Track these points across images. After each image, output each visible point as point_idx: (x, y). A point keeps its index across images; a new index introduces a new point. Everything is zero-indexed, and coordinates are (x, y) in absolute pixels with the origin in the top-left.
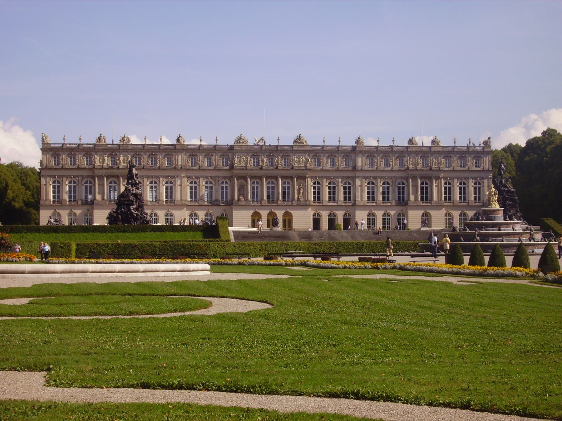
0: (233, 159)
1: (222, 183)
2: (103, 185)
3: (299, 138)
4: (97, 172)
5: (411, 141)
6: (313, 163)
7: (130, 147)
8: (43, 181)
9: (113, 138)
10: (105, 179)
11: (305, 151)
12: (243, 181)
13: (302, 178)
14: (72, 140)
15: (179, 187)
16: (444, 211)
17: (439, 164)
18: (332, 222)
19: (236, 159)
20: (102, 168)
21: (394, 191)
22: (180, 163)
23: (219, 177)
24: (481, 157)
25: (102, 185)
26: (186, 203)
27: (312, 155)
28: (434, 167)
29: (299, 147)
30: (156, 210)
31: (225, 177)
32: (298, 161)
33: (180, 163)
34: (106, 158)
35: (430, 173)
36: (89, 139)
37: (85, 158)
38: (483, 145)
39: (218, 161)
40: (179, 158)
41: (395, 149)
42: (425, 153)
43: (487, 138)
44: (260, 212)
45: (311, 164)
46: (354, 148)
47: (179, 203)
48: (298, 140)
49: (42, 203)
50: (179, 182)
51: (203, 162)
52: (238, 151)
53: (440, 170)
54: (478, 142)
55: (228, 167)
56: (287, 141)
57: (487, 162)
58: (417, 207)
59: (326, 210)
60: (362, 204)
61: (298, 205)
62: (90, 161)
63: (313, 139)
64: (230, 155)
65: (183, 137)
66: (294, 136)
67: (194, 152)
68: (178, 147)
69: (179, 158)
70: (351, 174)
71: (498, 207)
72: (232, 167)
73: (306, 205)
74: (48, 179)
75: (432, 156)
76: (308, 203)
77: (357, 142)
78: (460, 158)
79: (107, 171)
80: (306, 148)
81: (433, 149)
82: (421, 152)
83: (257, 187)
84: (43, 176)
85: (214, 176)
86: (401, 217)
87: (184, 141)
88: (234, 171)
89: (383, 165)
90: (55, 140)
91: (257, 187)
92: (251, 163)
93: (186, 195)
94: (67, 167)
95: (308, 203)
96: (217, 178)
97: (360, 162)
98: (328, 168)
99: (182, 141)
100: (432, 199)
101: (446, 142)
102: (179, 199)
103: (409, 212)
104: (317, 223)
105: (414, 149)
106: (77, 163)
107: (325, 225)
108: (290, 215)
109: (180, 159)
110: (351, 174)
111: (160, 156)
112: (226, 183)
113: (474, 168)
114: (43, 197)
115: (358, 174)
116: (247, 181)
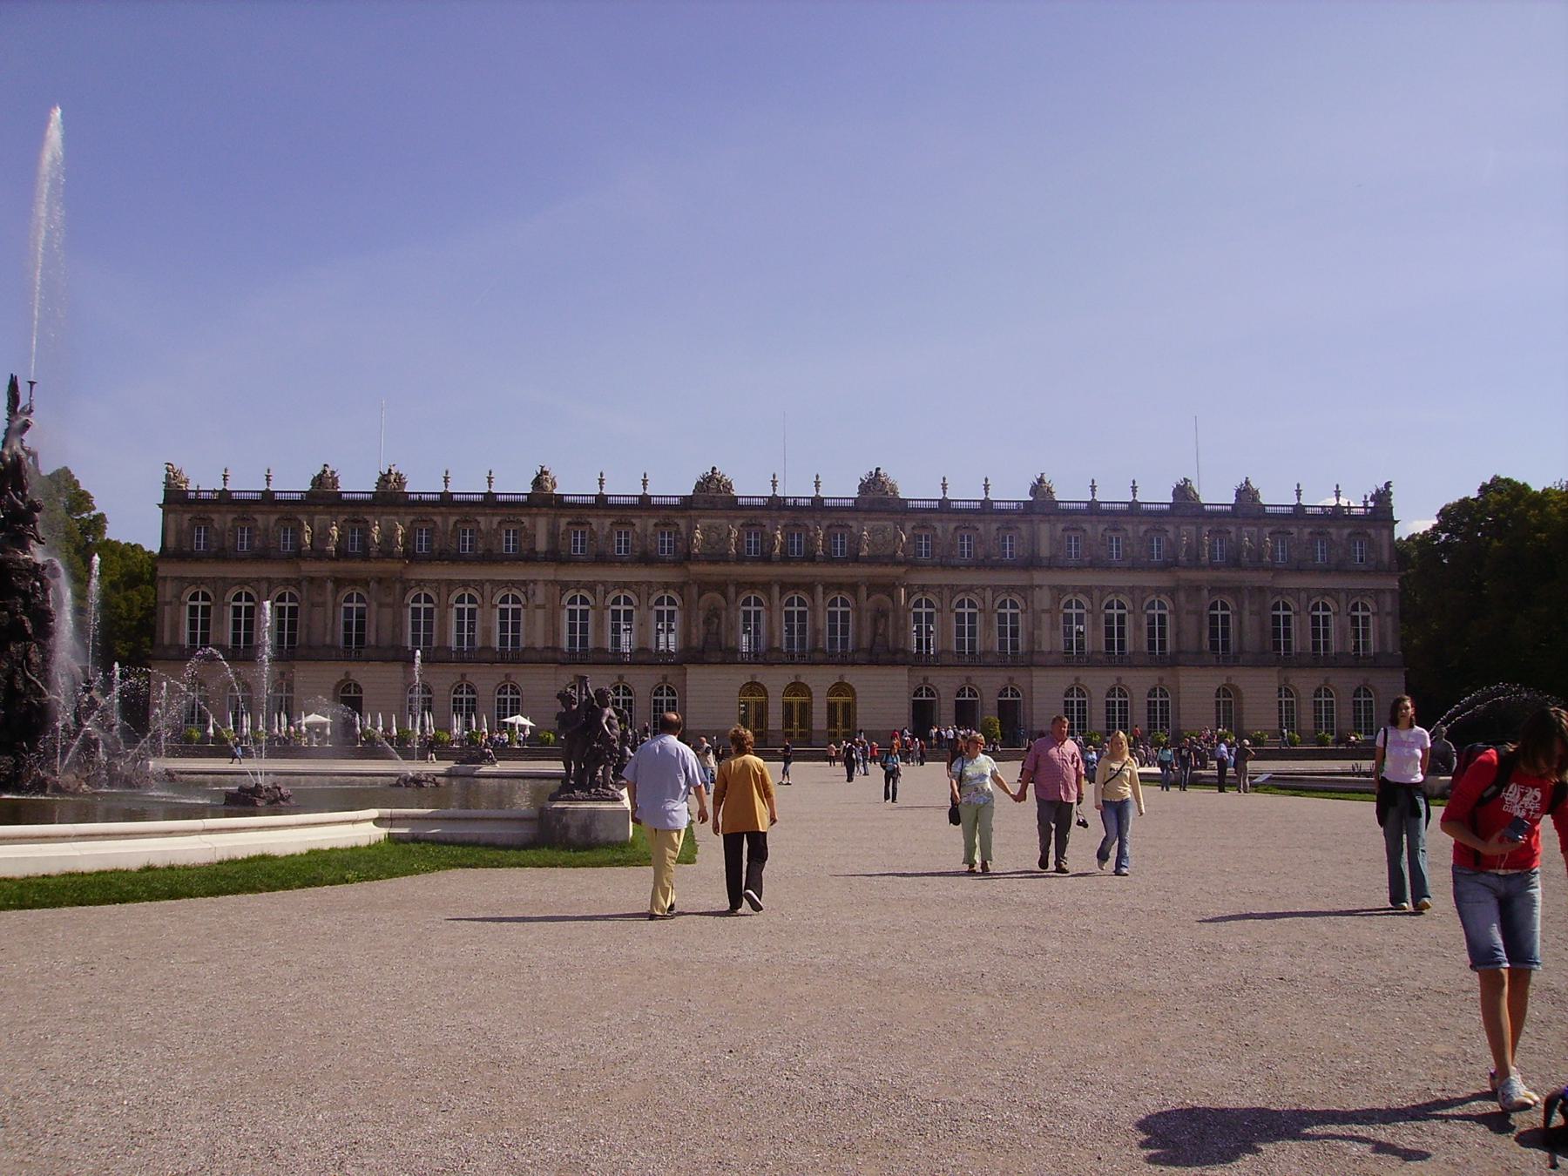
1: (660, 602)
21: (1138, 627)
22: (542, 545)
23: (650, 584)
26: (559, 656)
31: (667, 586)
33: (542, 545)
38: (1371, 504)
43: (1381, 486)
64: (682, 523)
65: (552, 474)
66: (863, 473)
76: (899, 657)
79: (331, 566)
83: (757, 613)
85: (636, 583)
86: (1117, 699)
87: (554, 486)
90: (202, 479)
91: (757, 613)
96: (644, 588)
98: (955, 561)
112: (671, 602)
115: (1039, 577)
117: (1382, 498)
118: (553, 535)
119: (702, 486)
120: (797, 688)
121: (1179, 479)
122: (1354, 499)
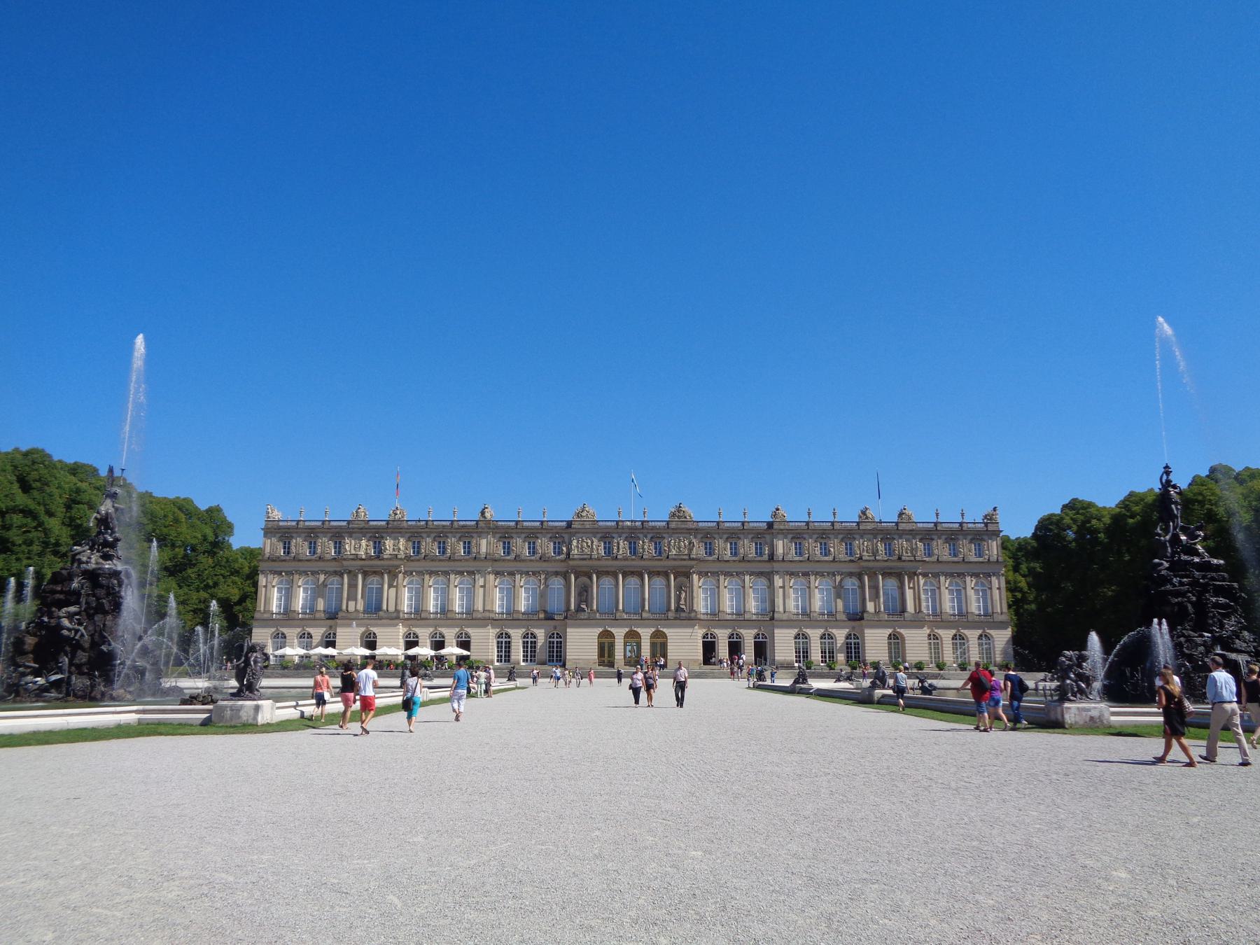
0: (570, 543)
2: (356, 586)
6: (703, 548)
7: (405, 524)
8: (262, 580)
10: (360, 576)
11: (689, 531)
12: (585, 579)
13: (684, 574)
15: (481, 590)
16: (926, 631)
17: (914, 550)
19: (575, 543)
20: (356, 558)
22: (483, 550)
24: (983, 540)
25: (353, 586)
26: (492, 615)
27: (700, 536)
28: (906, 556)
29: (679, 525)
30: (442, 626)
32: (675, 547)
33: (483, 550)
34: (364, 543)
37: (332, 544)
39: (546, 546)
40: (484, 542)
41: (837, 526)
42: (887, 534)
43: (989, 510)
44: (613, 630)
45: (699, 550)
46: (770, 525)
47: (480, 616)
48: (678, 513)
49: (257, 615)
50: (481, 582)
51: (521, 547)
52: (577, 532)
55: (563, 556)
56: (659, 514)
58: (879, 624)
59: (726, 628)
60: (785, 617)
61: (676, 619)
62: (339, 547)
63: (701, 512)
64: (566, 536)
67: (505, 533)
68: (481, 524)
69: (484, 542)
70: (766, 567)
73: (690, 619)
74: (270, 577)
75: (901, 537)
76: (693, 615)
77: (775, 515)
78: (947, 541)
80: (690, 525)
81: (902, 526)
82: (881, 531)
84: (263, 572)
88: (571, 563)
89: (818, 553)
92: (599, 548)
93: (492, 602)
94: (301, 557)
95: (693, 615)
97: (780, 546)
98: (726, 558)
99: (488, 515)
100: (904, 610)
102: (481, 609)
103: (866, 631)
105: (870, 526)
106: (319, 551)
108: (664, 636)
109: (484, 545)
111: (451, 541)
113: (973, 558)
114: (261, 606)
115: (776, 566)
116: (591, 578)
118: (488, 543)
119: (578, 515)
120: (632, 636)
121: (862, 508)
122: (974, 516)
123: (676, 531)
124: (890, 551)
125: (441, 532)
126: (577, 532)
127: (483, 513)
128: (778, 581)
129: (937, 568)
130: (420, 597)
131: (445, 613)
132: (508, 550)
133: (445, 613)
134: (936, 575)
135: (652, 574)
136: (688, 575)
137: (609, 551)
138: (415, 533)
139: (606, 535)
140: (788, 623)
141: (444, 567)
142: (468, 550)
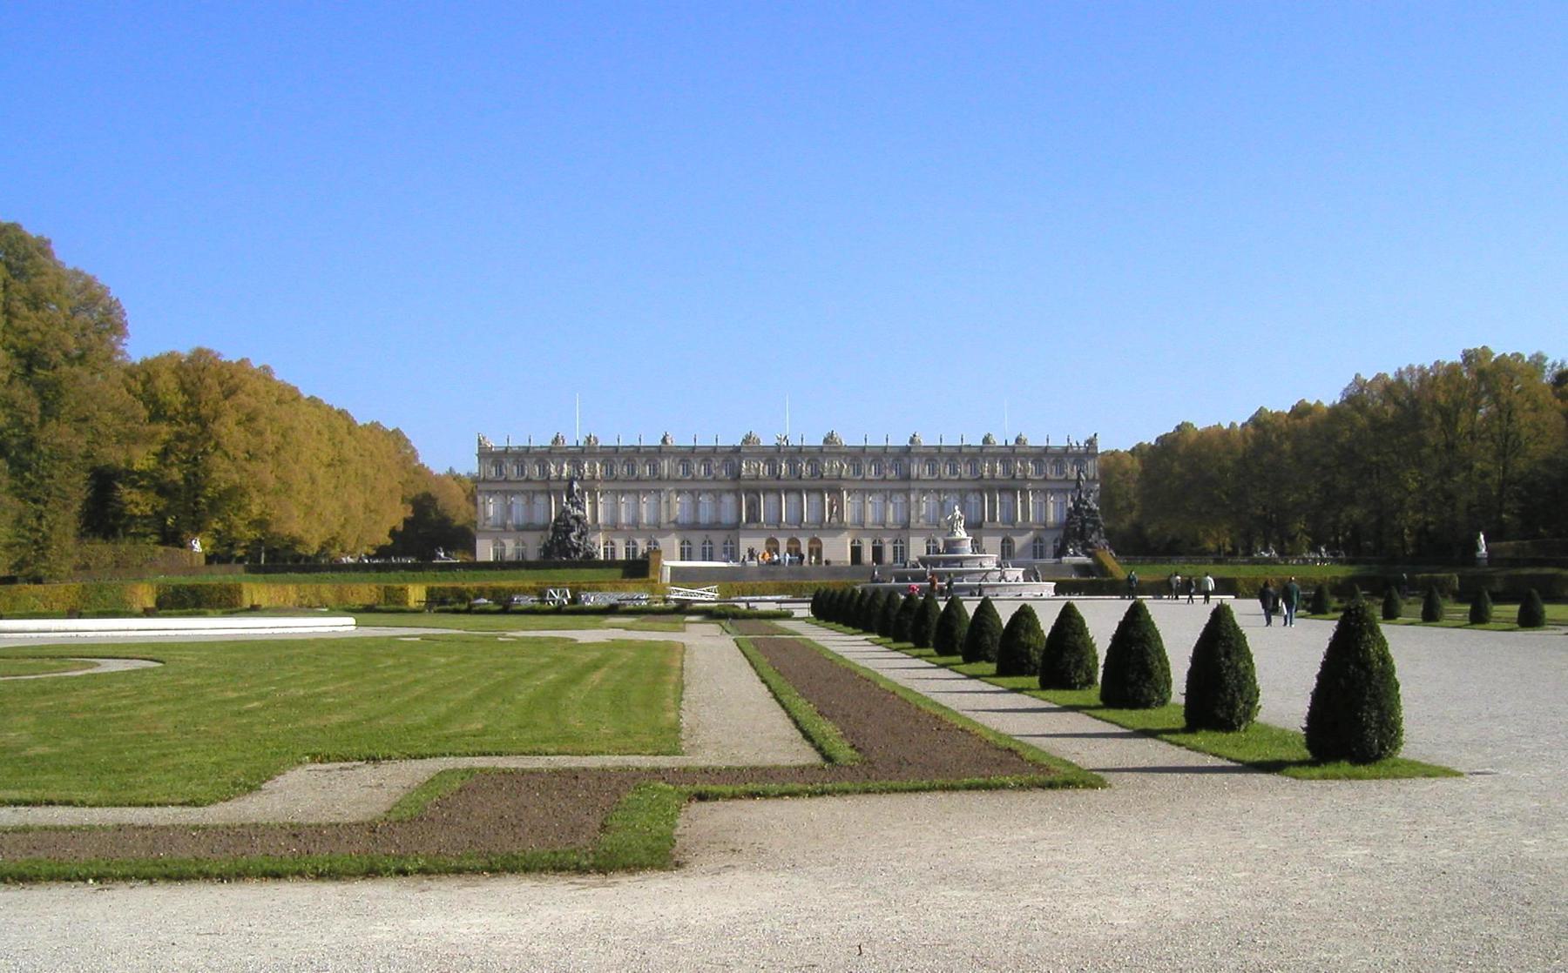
3: (831, 435)
4: (553, 485)
5: (986, 440)
8: (480, 499)
9: (574, 437)
11: (840, 454)
13: (836, 492)
14: (517, 442)
17: (1025, 470)
18: (878, 553)
32: (830, 467)
35: (1012, 484)
36: (543, 440)
48: (829, 439)
52: (746, 455)
53: (1026, 479)
54: (1079, 439)
57: (1092, 468)
71: (964, 535)
72: (737, 477)
77: (912, 441)
78: (1054, 463)
90: (496, 442)
92: (764, 469)
101: (1035, 440)
104: (856, 552)
107: (867, 556)
109: (666, 466)
110: (904, 485)
115: (913, 485)
117: (1091, 442)
123: (829, 454)
124: (1007, 470)
125: (634, 454)
126: (746, 455)
127: (664, 440)
128: (913, 498)
129: (1045, 486)
130: (615, 510)
131: (636, 524)
132: (687, 471)
133: (636, 524)
134: (1045, 492)
135: (809, 491)
136: (839, 492)
137: (773, 471)
138: (611, 455)
139: (773, 455)
140: (920, 531)
141: (634, 486)
142: (654, 470)
